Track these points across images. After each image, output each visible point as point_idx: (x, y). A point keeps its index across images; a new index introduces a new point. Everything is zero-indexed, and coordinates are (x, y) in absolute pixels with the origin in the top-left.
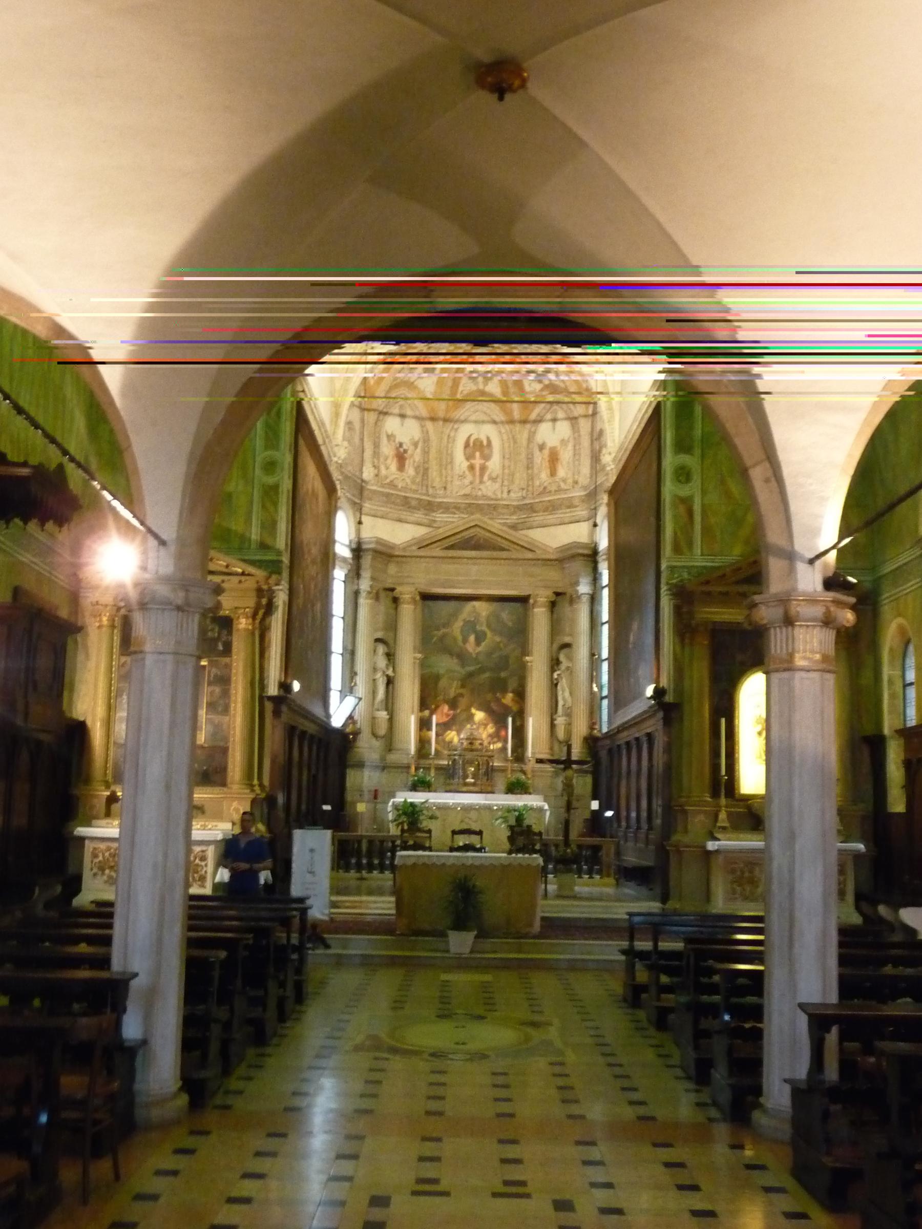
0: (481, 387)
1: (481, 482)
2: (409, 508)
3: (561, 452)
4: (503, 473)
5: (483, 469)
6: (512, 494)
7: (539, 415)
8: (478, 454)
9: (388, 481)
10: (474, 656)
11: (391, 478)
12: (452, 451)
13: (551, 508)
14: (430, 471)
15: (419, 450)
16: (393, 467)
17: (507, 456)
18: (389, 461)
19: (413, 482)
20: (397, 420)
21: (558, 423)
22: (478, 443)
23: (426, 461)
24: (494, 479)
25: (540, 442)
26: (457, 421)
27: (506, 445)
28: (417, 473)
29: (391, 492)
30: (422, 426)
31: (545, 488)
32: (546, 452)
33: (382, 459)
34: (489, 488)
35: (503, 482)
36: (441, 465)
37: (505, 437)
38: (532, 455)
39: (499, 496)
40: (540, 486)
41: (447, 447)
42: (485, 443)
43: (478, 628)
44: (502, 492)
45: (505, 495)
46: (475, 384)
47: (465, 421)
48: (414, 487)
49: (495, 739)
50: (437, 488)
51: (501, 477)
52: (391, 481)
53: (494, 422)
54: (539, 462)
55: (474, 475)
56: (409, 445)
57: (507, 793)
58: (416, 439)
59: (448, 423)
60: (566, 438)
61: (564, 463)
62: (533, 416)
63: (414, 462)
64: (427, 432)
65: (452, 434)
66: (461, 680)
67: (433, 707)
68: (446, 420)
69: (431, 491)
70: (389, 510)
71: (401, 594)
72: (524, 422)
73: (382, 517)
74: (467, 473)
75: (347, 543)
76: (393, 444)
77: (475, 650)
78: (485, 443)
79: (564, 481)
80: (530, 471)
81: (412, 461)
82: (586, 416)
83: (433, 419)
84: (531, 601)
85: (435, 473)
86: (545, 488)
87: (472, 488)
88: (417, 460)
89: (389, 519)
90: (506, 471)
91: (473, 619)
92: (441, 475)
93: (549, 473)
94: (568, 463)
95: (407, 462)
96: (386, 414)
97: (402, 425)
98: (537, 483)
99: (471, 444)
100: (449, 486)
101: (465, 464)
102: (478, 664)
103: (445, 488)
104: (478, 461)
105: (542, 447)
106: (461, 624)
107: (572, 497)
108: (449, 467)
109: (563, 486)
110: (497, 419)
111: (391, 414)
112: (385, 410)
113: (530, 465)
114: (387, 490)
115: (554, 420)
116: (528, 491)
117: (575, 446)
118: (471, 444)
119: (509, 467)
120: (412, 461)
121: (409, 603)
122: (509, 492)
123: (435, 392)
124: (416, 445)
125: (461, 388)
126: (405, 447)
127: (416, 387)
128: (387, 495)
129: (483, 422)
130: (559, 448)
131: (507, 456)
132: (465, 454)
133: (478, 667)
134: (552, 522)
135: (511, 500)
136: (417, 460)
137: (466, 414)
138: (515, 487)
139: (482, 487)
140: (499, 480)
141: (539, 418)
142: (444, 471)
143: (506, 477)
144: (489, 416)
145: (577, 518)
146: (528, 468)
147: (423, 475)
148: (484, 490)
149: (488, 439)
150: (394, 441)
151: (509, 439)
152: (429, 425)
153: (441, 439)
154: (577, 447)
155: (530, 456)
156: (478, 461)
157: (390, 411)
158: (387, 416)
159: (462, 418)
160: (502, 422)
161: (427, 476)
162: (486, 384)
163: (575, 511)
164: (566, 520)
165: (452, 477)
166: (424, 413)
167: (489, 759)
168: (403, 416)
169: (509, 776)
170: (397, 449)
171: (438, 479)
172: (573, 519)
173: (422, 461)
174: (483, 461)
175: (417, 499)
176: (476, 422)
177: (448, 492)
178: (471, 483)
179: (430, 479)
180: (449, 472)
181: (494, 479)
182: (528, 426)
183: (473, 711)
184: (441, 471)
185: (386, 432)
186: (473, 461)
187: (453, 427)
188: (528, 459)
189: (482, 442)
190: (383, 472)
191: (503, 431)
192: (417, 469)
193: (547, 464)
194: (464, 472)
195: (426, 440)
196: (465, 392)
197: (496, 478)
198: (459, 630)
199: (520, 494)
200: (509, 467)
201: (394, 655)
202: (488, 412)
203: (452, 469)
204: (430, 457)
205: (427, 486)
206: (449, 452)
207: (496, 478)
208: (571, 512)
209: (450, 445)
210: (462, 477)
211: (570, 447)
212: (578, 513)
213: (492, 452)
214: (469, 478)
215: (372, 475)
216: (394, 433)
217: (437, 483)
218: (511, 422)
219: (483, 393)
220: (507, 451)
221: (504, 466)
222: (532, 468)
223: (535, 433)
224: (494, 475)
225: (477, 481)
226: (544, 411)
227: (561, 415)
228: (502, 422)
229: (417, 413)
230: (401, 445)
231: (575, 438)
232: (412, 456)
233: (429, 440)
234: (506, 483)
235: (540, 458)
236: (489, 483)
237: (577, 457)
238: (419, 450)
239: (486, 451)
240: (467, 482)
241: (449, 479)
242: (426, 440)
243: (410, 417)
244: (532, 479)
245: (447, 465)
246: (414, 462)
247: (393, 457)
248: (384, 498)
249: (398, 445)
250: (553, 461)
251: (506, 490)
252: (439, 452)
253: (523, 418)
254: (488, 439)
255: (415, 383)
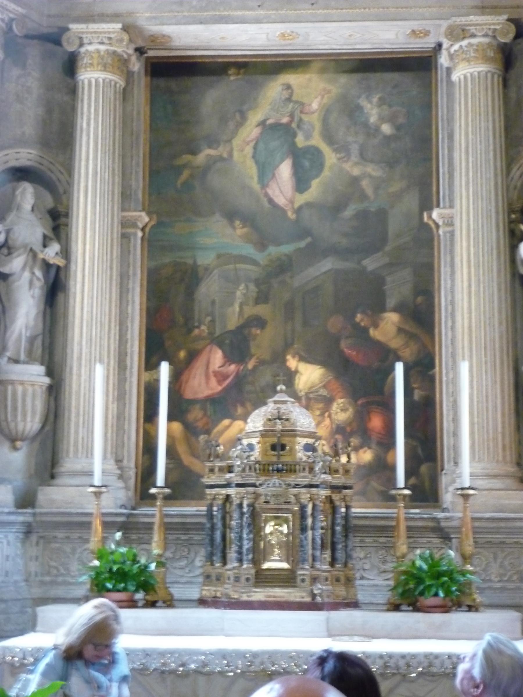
10: (291, 215)
43: (300, 141)
49: (355, 441)
57: (396, 608)
66: (257, 282)
67: (182, 354)
71: (81, 45)
77: (292, 202)
84: (444, 60)
91: (285, 120)
102: (300, 237)
106: (256, 132)
121: (105, 68)
133: (302, 244)
167: (336, 497)
169: (403, 548)
183: (292, 363)
198: (249, 150)
201: (67, 215)
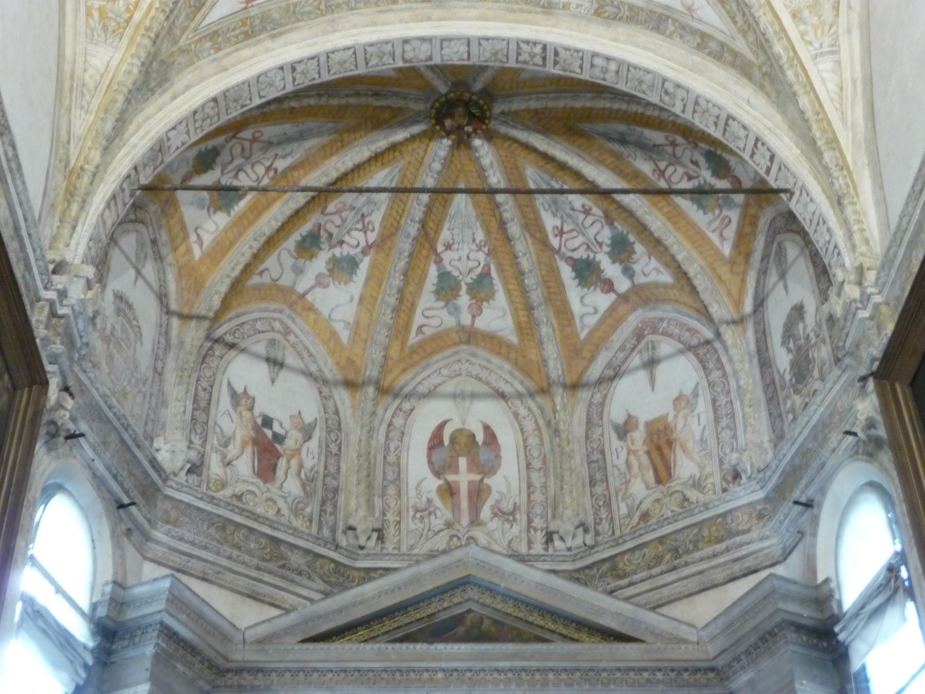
0: (466, 320)
1: (475, 521)
2: (283, 566)
3: (680, 425)
4: (529, 501)
5: (478, 493)
6: (558, 543)
7: (609, 365)
8: (463, 462)
9: (227, 493)
11: (240, 488)
12: (399, 458)
13: (668, 557)
14: (342, 497)
15: (313, 444)
16: (245, 465)
17: (537, 464)
18: (233, 450)
19: (296, 511)
20: (263, 369)
21: (663, 371)
22: (463, 439)
23: (332, 473)
24: (506, 515)
25: (620, 419)
26: (408, 396)
27: (533, 441)
28: (309, 495)
29: (238, 519)
30: (324, 398)
31: (645, 516)
32: (639, 436)
33: (213, 441)
34: (497, 535)
35: (530, 521)
36: (370, 486)
37: (529, 425)
38: (602, 452)
39: (523, 549)
40: (630, 515)
41: (387, 448)
42: (480, 438)
44: (530, 543)
45: (538, 549)
46: (450, 313)
47: (429, 395)
48: (298, 523)
50: (360, 527)
51: (524, 508)
52: (239, 497)
53: (502, 396)
54: (621, 462)
55: (456, 508)
56: (287, 425)
58: (308, 418)
59: (388, 399)
60: (688, 391)
61: (690, 445)
62: (595, 371)
63: (301, 466)
64: (337, 413)
65: (398, 422)
68: (383, 391)
69: (343, 541)
70: (224, 562)
72: (575, 387)
73: (204, 579)
74: (438, 502)
75: (85, 606)
76: (247, 415)
78: (480, 438)
79: (697, 484)
80: (599, 489)
81: (294, 463)
82: (739, 322)
83: (350, 385)
85: (353, 504)
86: (645, 516)
87: (452, 537)
88: (308, 463)
89: (221, 586)
90: (538, 497)
92: (371, 508)
93: (650, 475)
94: (703, 441)
95: (282, 463)
96: (232, 346)
97: (273, 382)
98: (624, 510)
99: (446, 442)
100: (391, 531)
101: (433, 484)
103: (381, 538)
104: (464, 478)
105: (624, 430)
107: (724, 515)
108: (392, 491)
109: (693, 495)
110: (507, 389)
111: (243, 350)
112: (229, 339)
113: (598, 476)
114: (221, 512)
115: (651, 364)
116: (597, 534)
117: (714, 401)
118: (446, 442)
119: (544, 486)
120: (294, 463)
122: (549, 538)
123: (357, 323)
124: (307, 432)
125: (418, 320)
126: (276, 427)
127: (311, 308)
128: (224, 524)
129: (473, 396)
130: (670, 419)
131: (537, 464)
132: (430, 462)
134: (677, 588)
135: (554, 558)
136: (308, 463)
137: (435, 380)
138: (565, 525)
139: (477, 533)
140: (522, 517)
141: (611, 372)
142: (378, 502)
143: (538, 510)
144: (488, 384)
145: (749, 563)
146: (592, 483)
147: (323, 503)
148: (482, 539)
149: (487, 428)
150: (251, 409)
151: (538, 428)
152: (342, 396)
153: (371, 431)
154: (722, 400)
155: (596, 456)
156: (464, 478)
157: (243, 344)
158: (233, 353)
159: (422, 389)
160: (520, 396)
161: (335, 507)
162: (476, 311)
163: (741, 545)
164: (719, 576)
165: (400, 513)
166: (330, 370)
168: (276, 364)
170: (256, 428)
171: (362, 513)
172: (737, 568)
173: (322, 469)
174: (476, 477)
175: (307, 552)
176: (454, 396)
177: (390, 547)
178: (449, 525)
179: (341, 515)
180: (392, 504)
181: (506, 515)
182: (584, 395)
184: (370, 501)
185: (229, 384)
186: (451, 478)
187: (399, 408)
188: (589, 463)
189: (473, 436)
190: (215, 467)
191: (523, 412)
192: (307, 484)
193: (645, 460)
194: (429, 501)
195: (334, 427)
196: (428, 331)
197: (512, 513)
199: (579, 541)
200: (544, 486)
202: (484, 374)
203: (399, 495)
204: (343, 466)
205: (333, 530)
206: (392, 458)
207: (512, 513)
208: (728, 550)
209: (392, 447)
210: (425, 511)
211: (703, 406)
212: (753, 547)
213: (498, 457)
214: (444, 512)
215: (180, 460)
216: (251, 392)
217: (361, 520)
218: (545, 391)
219: (470, 336)
220: (536, 453)
221: (530, 485)
222: (605, 478)
223: (602, 404)
224: (507, 506)
225: (465, 521)
226: (621, 355)
227: (666, 347)
228: (520, 396)
229: (313, 368)
230: (267, 422)
231: (711, 385)
232: (298, 451)
233: (340, 429)
234: (538, 522)
235: (623, 455)
236: (494, 524)
237: (724, 422)
238: (313, 444)
239: (484, 455)
240: (437, 523)
241: (391, 517)
242: (334, 427)
243: (292, 369)
244: (608, 504)
245: (384, 488)
246: (301, 466)
247: (244, 444)
248: (212, 531)
249: (259, 421)
250: (659, 449)
251: (539, 537)
252: (367, 456)
253: (568, 381)
254: (487, 428)
255: (309, 297)
